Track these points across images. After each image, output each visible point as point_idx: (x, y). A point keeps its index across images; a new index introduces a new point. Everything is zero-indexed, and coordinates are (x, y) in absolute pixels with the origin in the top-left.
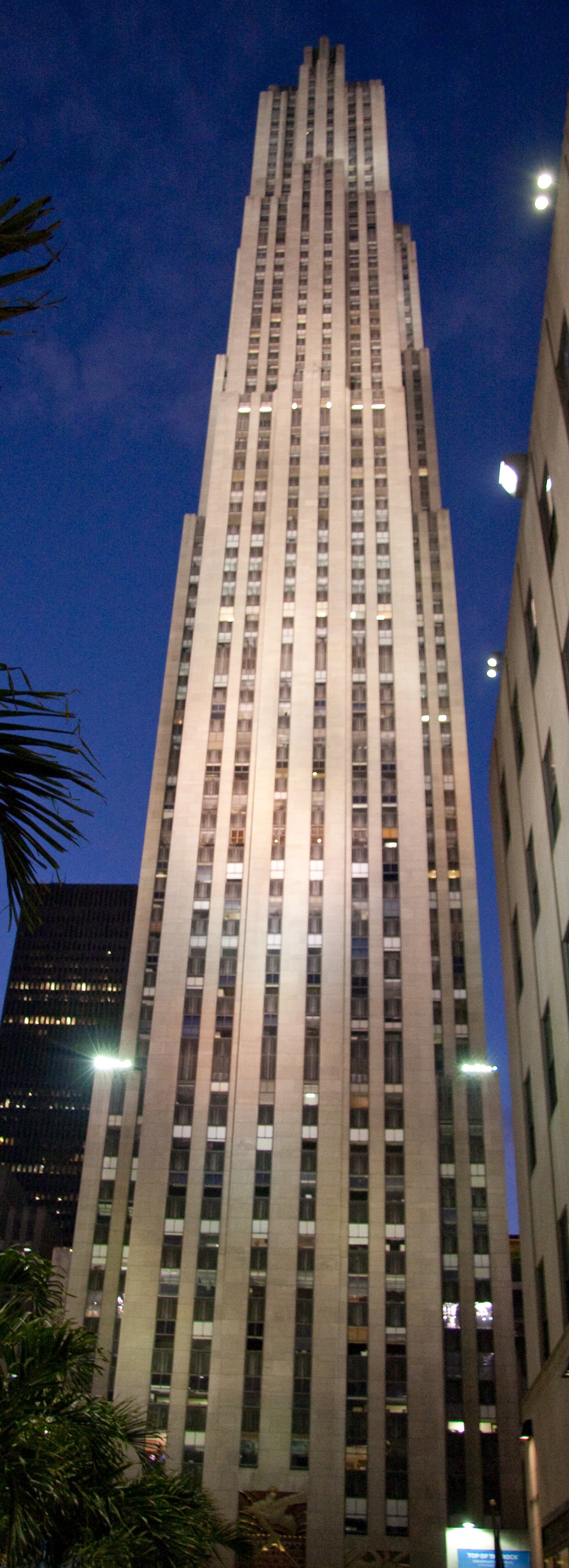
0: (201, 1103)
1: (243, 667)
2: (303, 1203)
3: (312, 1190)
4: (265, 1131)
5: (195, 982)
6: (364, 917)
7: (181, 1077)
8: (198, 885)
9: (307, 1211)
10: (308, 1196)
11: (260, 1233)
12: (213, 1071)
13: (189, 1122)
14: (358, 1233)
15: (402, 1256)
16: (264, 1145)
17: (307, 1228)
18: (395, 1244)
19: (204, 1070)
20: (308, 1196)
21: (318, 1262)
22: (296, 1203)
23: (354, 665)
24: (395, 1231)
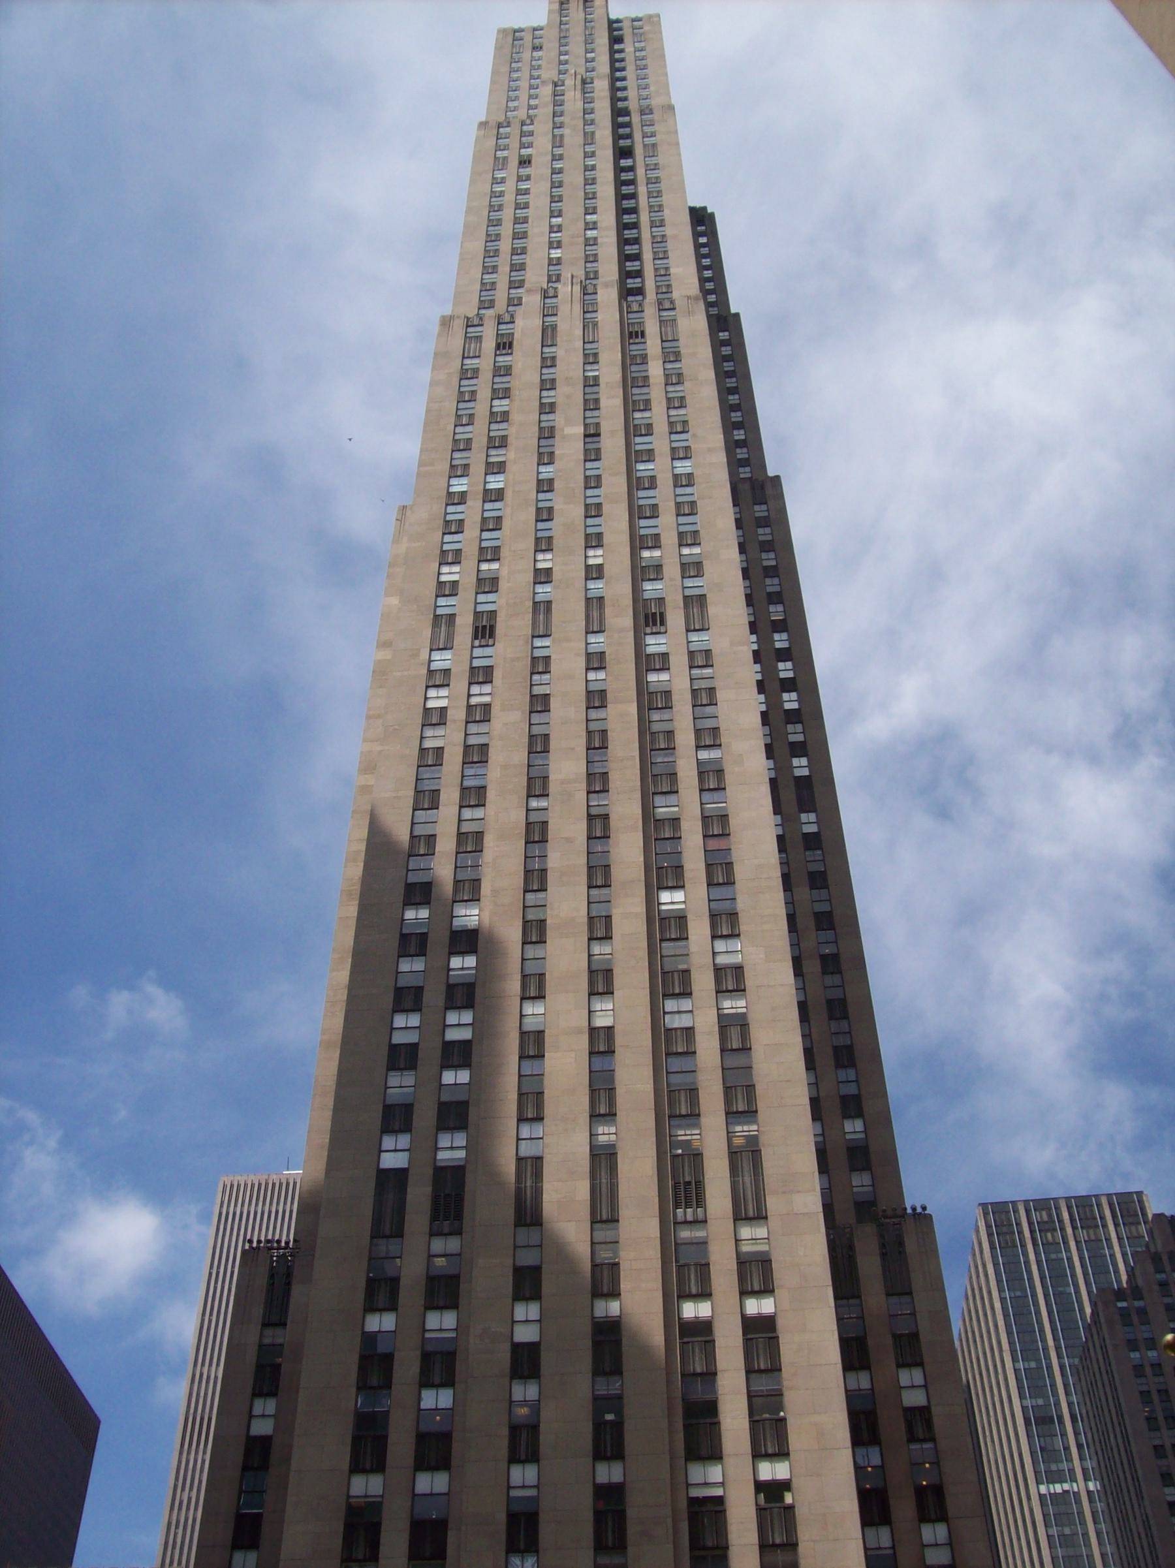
2: (599, 1426)
3: (615, 1402)
4: (526, 1311)
11: (524, 1487)
16: (525, 1334)
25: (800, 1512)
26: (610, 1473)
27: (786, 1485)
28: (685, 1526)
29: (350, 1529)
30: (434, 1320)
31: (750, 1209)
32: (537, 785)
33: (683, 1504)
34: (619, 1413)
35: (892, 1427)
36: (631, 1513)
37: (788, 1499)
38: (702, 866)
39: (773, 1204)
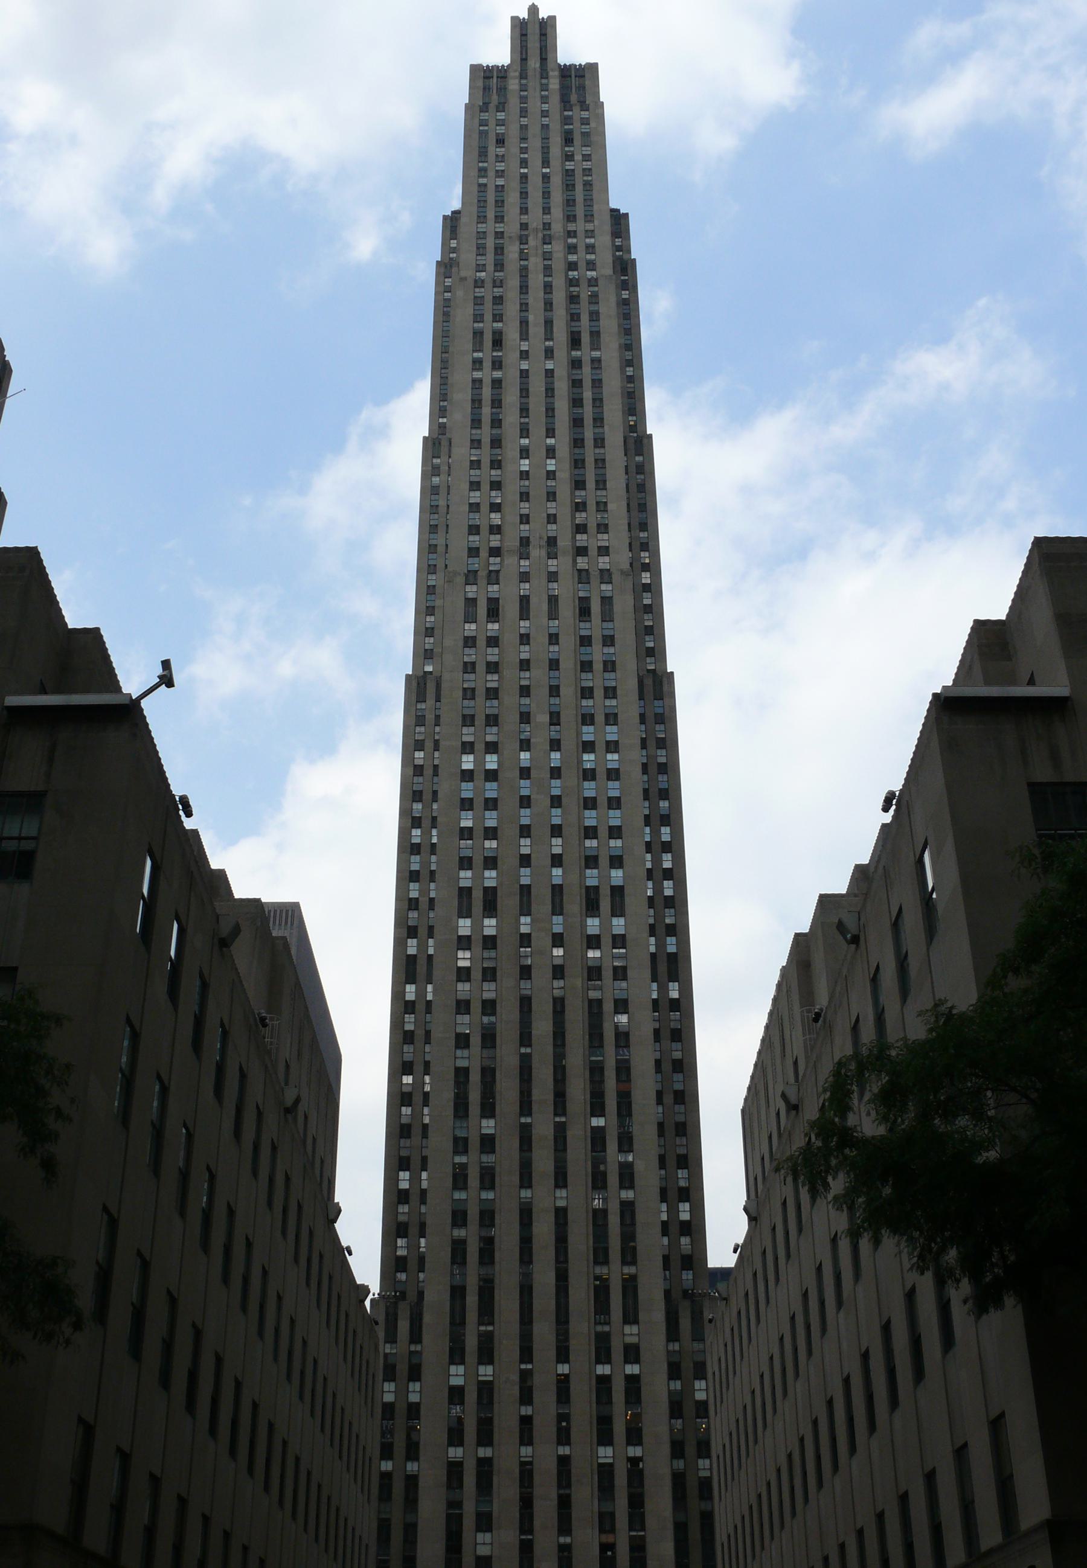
0: (471, 1343)
1: (485, 909)
2: (560, 1429)
5: (459, 1233)
6: (602, 1168)
7: (452, 1324)
8: (456, 1139)
9: (564, 1437)
10: (564, 1424)
12: (480, 1315)
13: (462, 1362)
14: (605, 1454)
15: (641, 1471)
17: (564, 1450)
18: (634, 1461)
19: (472, 1316)
20: (564, 1424)
21: (573, 1479)
22: (555, 1429)
23: (587, 910)
24: (635, 1451)
25: (646, 1473)
26: (564, 1450)
27: (640, 1459)
28: (596, 1477)
29: (450, 1474)
30: (482, 1370)
31: (631, 1316)
32: (525, 1038)
33: (595, 1466)
34: (568, 1423)
35: (689, 1410)
36: (573, 1471)
37: (641, 1466)
38: (615, 1103)
39: (642, 1316)
